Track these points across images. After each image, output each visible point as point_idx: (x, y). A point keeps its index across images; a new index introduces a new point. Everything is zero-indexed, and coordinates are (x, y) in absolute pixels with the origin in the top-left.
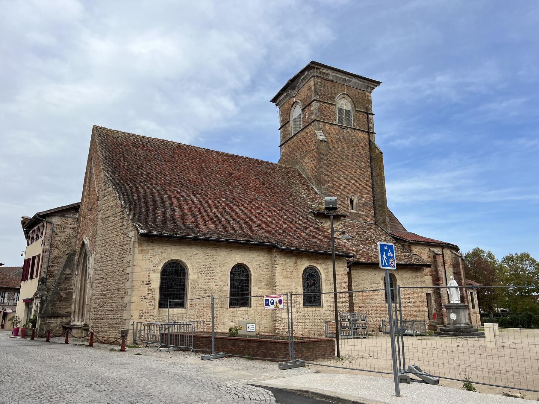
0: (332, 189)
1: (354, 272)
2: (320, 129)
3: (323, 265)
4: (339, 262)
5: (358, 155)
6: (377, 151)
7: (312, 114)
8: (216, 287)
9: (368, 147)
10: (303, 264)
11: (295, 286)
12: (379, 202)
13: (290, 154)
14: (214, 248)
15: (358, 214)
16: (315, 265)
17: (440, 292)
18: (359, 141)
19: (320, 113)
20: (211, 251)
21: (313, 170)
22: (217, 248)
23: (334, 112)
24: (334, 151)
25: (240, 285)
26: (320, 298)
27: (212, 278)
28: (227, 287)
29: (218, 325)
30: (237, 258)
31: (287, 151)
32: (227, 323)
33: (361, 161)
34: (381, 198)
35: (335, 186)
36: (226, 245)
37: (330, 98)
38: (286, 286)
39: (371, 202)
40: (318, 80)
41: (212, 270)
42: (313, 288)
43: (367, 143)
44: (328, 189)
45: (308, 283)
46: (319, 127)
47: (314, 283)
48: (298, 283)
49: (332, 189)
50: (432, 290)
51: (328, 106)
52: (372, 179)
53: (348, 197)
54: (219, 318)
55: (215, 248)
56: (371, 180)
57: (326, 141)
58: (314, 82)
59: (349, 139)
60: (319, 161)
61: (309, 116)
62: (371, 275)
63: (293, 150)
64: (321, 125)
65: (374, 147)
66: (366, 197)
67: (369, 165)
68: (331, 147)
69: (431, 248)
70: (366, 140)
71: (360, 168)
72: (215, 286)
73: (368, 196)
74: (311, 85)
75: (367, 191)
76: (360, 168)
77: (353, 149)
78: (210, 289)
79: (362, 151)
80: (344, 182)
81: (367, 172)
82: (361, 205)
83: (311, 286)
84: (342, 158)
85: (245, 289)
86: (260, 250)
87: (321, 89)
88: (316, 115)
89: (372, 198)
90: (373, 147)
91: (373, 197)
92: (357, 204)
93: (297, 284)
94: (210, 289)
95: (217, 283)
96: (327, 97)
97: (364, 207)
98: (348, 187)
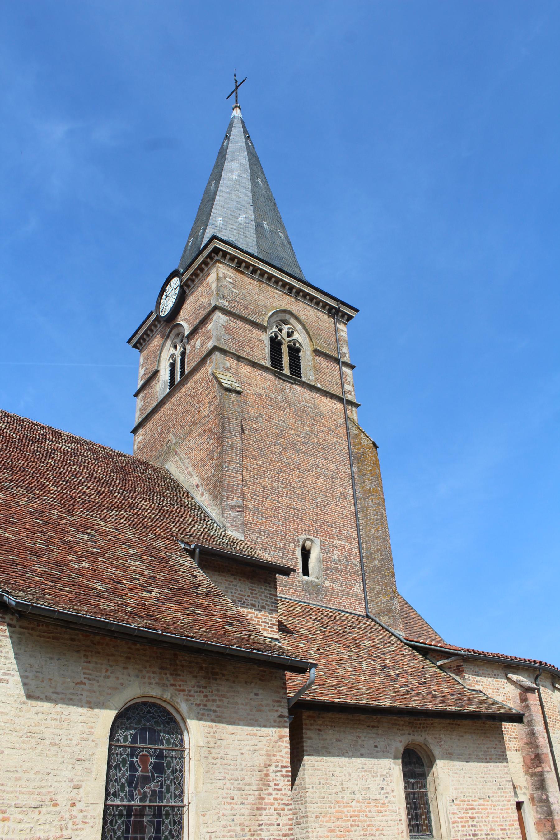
0: (254, 515)
1: (310, 738)
2: (227, 369)
3: (199, 699)
4: (260, 691)
5: (320, 445)
6: (365, 441)
7: (209, 338)
9: (343, 431)
10: (115, 689)
11: (70, 776)
12: (374, 559)
13: (155, 441)
15: (323, 587)
16: (167, 696)
17: (548, 797)
18: (321, 414)
19: (227, 337)
21: (206, 464)
23: (262, 341)
24: (262, 423)
26: (181, 828)
31: (148, 437)
33: (327, 459)
34: (378, 550)
35: (262, 509)
37: (254, 312)
38: (26, 776)
39: (356, 560)
40: (227, 272)
42: (152, 786)
43: (341, 421)
44: (240, 507)
45: (133, 768)
46: (225, 364)
47: (158, 768)
48: (87, 764)
49: (254, 515)
50: (525, 794)
51: (248, 327)
52: (355, 504)
53: (295, 541)
56: (353, 508)
57: (239, 393)
58: (218, 274)
59: (298, 405)
60: (220, 438)
61: (202, 346)
62: (362, 746)
63: (162, 430)
64: (230, 362)
65: (357, 432)
66: (343, 546)
67: (348, 471)
68: (252, 413)
69: (510, 676)
70: (338, 415)
71: (325, 476)
73: (346, 544)
74: (210, 282)
75: (344, 532)
76: (325, 476)
77: (308, 429)
79: (329, 438)
80: (285, 501)
81: (343, 485)
82: (330, 565)
83: (146, 780)
84: (280, 444)
87: (233, 290)
88: (218, 339)
89: (356, 551)
90: (354, 431)
91: (360, 548)
92: (319, 560)
93: (80, 767)
96: (246, 308)
97: (336, 570)
98: (296, 516)
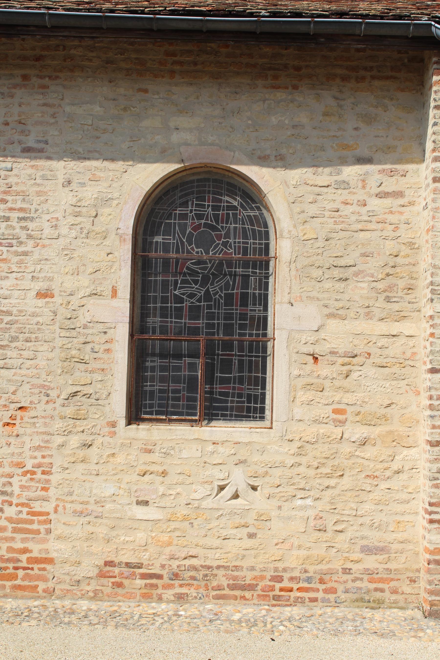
8: (41, 302)
14: (25, 77)
20: (12, 96)
22: (46, 81)
25: (208, 296)
27: (17, 254)
28: (115, 303)
29: (52, 516)
30: (175, 138)
32: (108, 506)
36: (109, 62)
41: (19, 205)
54: (55, 478)
55: (35, 80)
72: (40, 295)
78: (9, 313)
85: (243, 317)
86: (344, 79)
94: (9, 313)
95: (51, 279)
